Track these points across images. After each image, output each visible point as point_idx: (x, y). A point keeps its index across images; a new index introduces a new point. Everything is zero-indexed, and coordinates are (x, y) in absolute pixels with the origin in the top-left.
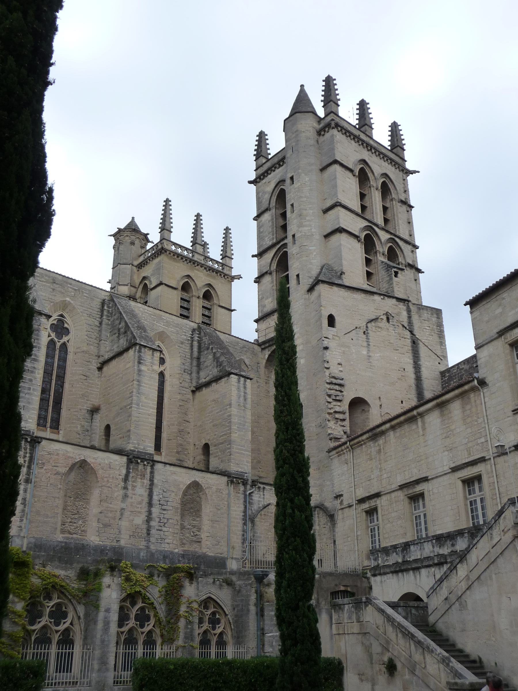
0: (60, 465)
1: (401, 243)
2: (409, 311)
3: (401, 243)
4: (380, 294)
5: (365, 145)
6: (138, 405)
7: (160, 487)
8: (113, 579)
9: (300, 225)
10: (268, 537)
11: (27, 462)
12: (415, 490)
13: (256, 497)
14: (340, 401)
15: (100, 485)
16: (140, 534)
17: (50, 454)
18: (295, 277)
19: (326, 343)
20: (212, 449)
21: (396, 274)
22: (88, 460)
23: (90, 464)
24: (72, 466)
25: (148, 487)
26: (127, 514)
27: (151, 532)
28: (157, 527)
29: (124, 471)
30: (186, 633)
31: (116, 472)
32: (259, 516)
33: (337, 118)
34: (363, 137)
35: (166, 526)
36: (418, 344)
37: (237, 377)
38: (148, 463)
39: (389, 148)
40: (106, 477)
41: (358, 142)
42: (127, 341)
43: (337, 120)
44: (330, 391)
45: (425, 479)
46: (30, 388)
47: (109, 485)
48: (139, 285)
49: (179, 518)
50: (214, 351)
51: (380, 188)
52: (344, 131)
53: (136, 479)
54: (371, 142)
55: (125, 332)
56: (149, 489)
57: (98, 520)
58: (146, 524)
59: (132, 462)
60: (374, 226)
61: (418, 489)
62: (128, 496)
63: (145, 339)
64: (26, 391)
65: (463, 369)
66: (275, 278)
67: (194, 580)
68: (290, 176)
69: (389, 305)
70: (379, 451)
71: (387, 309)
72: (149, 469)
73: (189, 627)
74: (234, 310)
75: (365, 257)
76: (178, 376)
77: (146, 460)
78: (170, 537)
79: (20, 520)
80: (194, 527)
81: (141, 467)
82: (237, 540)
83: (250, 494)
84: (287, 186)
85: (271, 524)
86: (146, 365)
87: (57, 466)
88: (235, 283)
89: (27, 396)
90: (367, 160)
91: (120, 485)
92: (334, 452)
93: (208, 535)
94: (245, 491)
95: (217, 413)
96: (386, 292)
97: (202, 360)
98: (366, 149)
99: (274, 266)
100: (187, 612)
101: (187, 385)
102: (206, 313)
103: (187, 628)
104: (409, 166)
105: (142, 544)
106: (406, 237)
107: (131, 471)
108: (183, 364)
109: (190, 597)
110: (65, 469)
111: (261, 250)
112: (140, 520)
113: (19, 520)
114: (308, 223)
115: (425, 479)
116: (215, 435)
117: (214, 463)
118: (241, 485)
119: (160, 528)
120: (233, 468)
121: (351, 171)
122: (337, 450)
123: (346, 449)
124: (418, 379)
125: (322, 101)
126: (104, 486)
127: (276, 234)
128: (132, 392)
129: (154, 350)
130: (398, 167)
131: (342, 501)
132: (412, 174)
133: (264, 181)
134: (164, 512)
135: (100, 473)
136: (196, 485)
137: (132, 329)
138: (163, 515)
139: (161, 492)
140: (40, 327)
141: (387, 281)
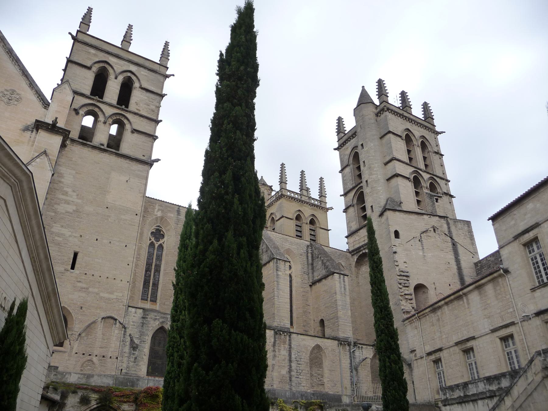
1: (438, 179)
2: (448, 224)
3: (438, 179)
4: (428, 215)
5: (407, 119)
6: (278, 297)
7: (295, 349)
9: (371, 174)
10: (368, 381)
12: (466, 346)
13: (357, 353)
14: (407, 287)
16: (285, 381)
18: (370, 207)
19: (394, 249)
20: (326, 323)
21: (437, 200)
25: (288, 350)
26: (276, 367)
27: (292, 379)
28: (296, 376)
32: (360, 366)
33: (388, 104)
34: (405, 114)
35: (301, 375)
36: (457, 245)
37: (338, 275)
38: (287, 334)
39: (423, 119)
41: (403, 118)
42: (268, 256)
43: (388, 106)
44: (400, 281)
45: (473, 338)
48: (269, 218)
49: (309, 369)
50: (322, 259)
51: (420, 145)
52: (393, 112)
54: (411, 117)
55: (267, 251)
56: (289, 351)
59: (277, 334)
60: (418, 170)
61: (469, 344)
62: (276, 356)
63: (279, 255)
65: (490, 260)
66: (356, 209)
68: (361, 144)
69: (434, 221)
70: (438, 320)
71: (433, 224)
72: (288, 337)
74: (330, 230)
75: (415, 191)
76: (300, 276)
77: (286, 332)
78: (304, 382)
80: (319, 375)
81: (283, 337)
82: (347, 383)
83: (353, 351)
84: (359, 150)
85: (368, 371)
86: (281, 271)
88: (329, 213)
90: (410, 129)
92: (407, 321)
93: (328, 380)
94: (350, 350)
95: (327, 299)
96: (431, 213)
97: (314, 265)
98: (408, 122)
99: (355, 201)
101: (306, 282)
102: (313, 233)
104: (438, 129)
105: (287, 387)
106: (441, 175)
108: (303, 268)
111: (346, 191)
112: (284, 371)
114: (375, 173)
115: (473, 338)
116: (327, 313)
117: (328, 332)
118: (347, 346)
119: (297, 376)
120: (341, 335)
121: (400, 136)
122: (409, 320)
123: (415, 319)
124: (459, 269)
125: (377, 95)
127: (355, 180)
128: (274, 289)
129: (285, 261)
130: (431, 131)
131: (416, 354)
132: (440, 134)
133: (344, 148)
134: (299, 366)
136: (318, 347)
137: (271, 249)
139: (296, 352)
141: (431, 205)
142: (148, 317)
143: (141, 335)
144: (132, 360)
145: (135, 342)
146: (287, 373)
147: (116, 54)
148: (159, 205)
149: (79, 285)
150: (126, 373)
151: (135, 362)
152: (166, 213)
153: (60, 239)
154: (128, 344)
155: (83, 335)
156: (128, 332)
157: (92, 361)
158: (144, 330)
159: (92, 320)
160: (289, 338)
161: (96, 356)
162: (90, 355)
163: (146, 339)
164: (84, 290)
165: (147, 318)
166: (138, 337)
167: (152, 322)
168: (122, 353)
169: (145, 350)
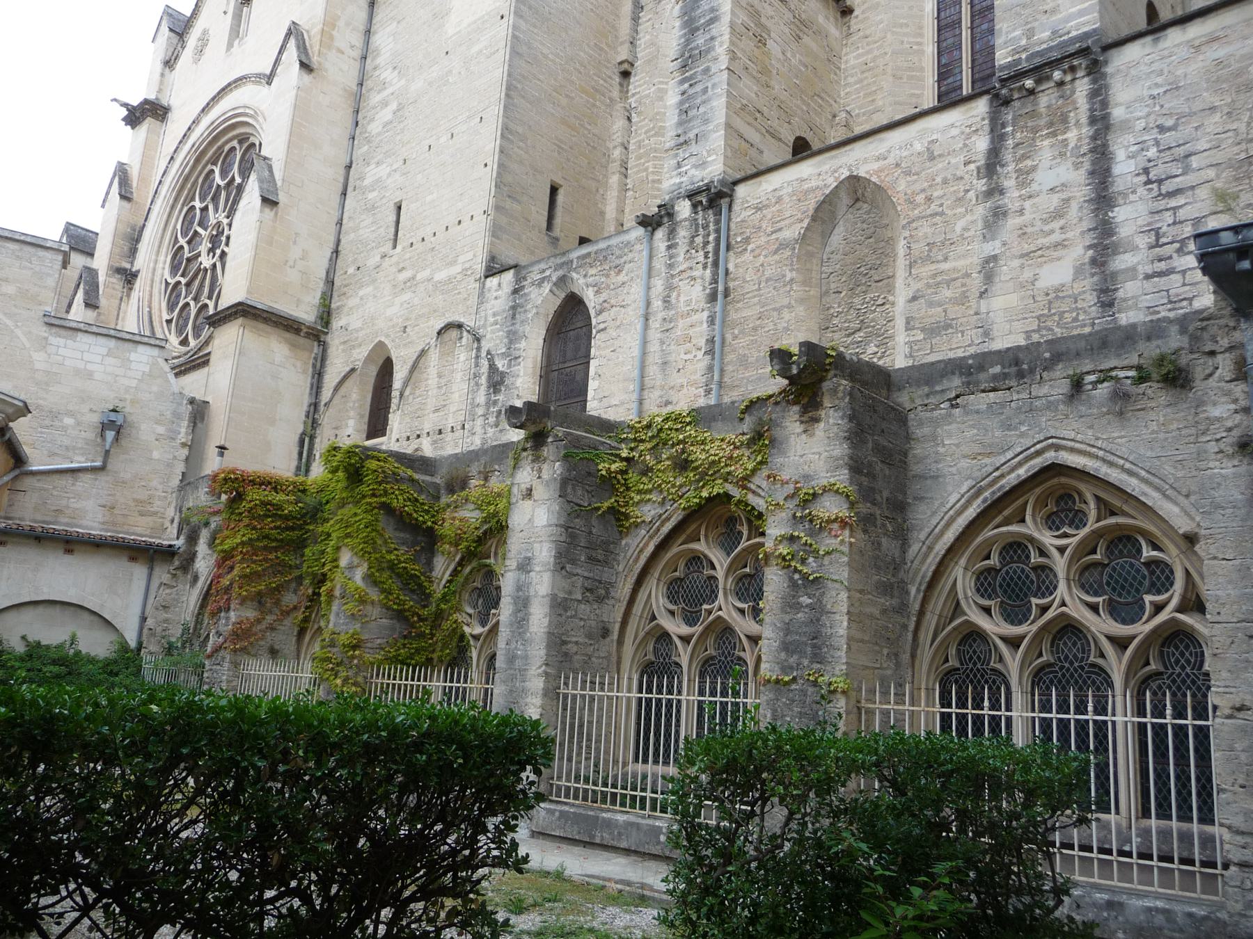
0: (787, 222)
8: (540, 470)
15: (905, 222)
17: (760, 209)
22: (862, 173)
23: (869, 181)
24: (817, 210)
25: (1085, 149)
26: (1006, 270)
27: (1120, 294)
29: (982, 144)
30: (787, 629)
31: (953, 161)
38: (1073, 69)
40: (923, 190)
47: (934, 207)
53: (1033, 145)
57: (908, 323)
58: (1093, 275)
59: (1007, 102)
67: (827, 403)
72: (1082, 87)
73: (805, 600)
91: (971, 194)
100: (792, 539)
103: (797, 607)
107: (1009, 129)
109: (807, 477)
110: (799, 226)
119: (1162, 266)
126: (919, 218)
134: (1173, 203)
135: (901, 188)
138: (1169, 213)
143: (511, 342)
146: (1078, 272)
153: (375, 194)
154: (483, 380)
155: (407, 393)
156: (485, 345)
160: (1094, 81)
169: (519, 382)
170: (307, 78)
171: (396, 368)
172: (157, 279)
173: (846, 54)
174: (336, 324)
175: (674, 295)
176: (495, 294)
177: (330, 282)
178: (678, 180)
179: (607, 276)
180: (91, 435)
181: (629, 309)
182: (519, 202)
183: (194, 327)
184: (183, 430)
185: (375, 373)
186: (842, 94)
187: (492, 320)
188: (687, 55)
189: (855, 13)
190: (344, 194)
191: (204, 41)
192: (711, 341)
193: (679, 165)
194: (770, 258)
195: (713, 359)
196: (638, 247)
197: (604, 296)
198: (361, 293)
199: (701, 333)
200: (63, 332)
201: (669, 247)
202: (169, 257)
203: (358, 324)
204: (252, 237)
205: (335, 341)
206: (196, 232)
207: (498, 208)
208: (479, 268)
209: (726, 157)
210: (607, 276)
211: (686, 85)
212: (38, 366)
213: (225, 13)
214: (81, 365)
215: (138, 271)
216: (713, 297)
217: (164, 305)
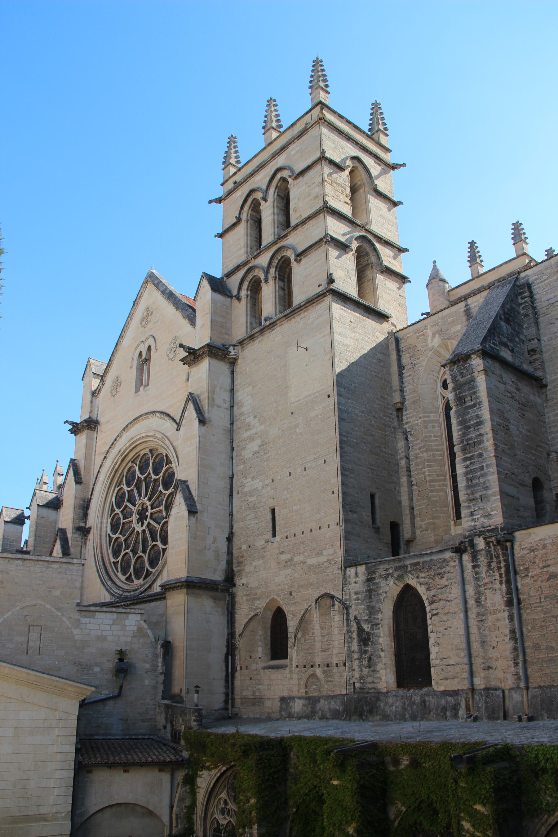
11: (503, 576)
17: (533, 551)
46: (483, 466)
64: (478, 474)
79: (514, 663)
87: (548, 566)
89: (482, 480)
113: (513, 665)
140: (473, 375)
142: (375, 576)
144: (365, 663)
145: (364, 629)
147: (257, 167)
148: (432, 326)
149: (284, 557)
150: (360, 688)
151: (370, 667)
152: (447, 332)
154: (355, 635)
155: (299, 635)
156: (353, 613)
157: (316, 676)
158: (374, 604)
159: (305, 608)
161: (319, 665)
162: (312, 666)
163: (378, 619)
164: (289, 563)
165: (374, 578)
166: (366, 618)
167: (383, 583)
168: (350, 653)
169: (381, 640)
170: (204, 429)
171: (289, 618)
172: (104, 534)
173: (548, 413)
174: (239, 581)
175: (483, 598)
176: (354, 580)
177: (230, 553)
178: (473, 524)
179: (433, 579)
180: (109, 676)
181: (453, 603)
182: (355, 512)
183: (135, 569)
184: (160, 664)
185: (271, 617)
186: (550, 438)
187: (354, 597)
188: (465, 443)
189: (549, 388)
190: (231, 495)
191: (117, 384)
192: (513, 631)
193: (472, 514)
194: (544, 584)
195: (516, 643)
196: (452, 564)
197: (432, 593)
198: (254, 563)
199: (505, 626)
200: (87, 614)
201: (474, 567)
202: (109, 520)
203: (255, 584)
204: (185, 535)
205: (240, 593)
206: (126, 506)
207: (346, 521)
208: (339, 560)
209: (503, 512)
210: (433, 579)
211: (468, 462)
212: (77, 637)
213: (131, 368)
214: (99, 633)
215: (90, 528)
216: (509, 603)
217: (110, 551)
